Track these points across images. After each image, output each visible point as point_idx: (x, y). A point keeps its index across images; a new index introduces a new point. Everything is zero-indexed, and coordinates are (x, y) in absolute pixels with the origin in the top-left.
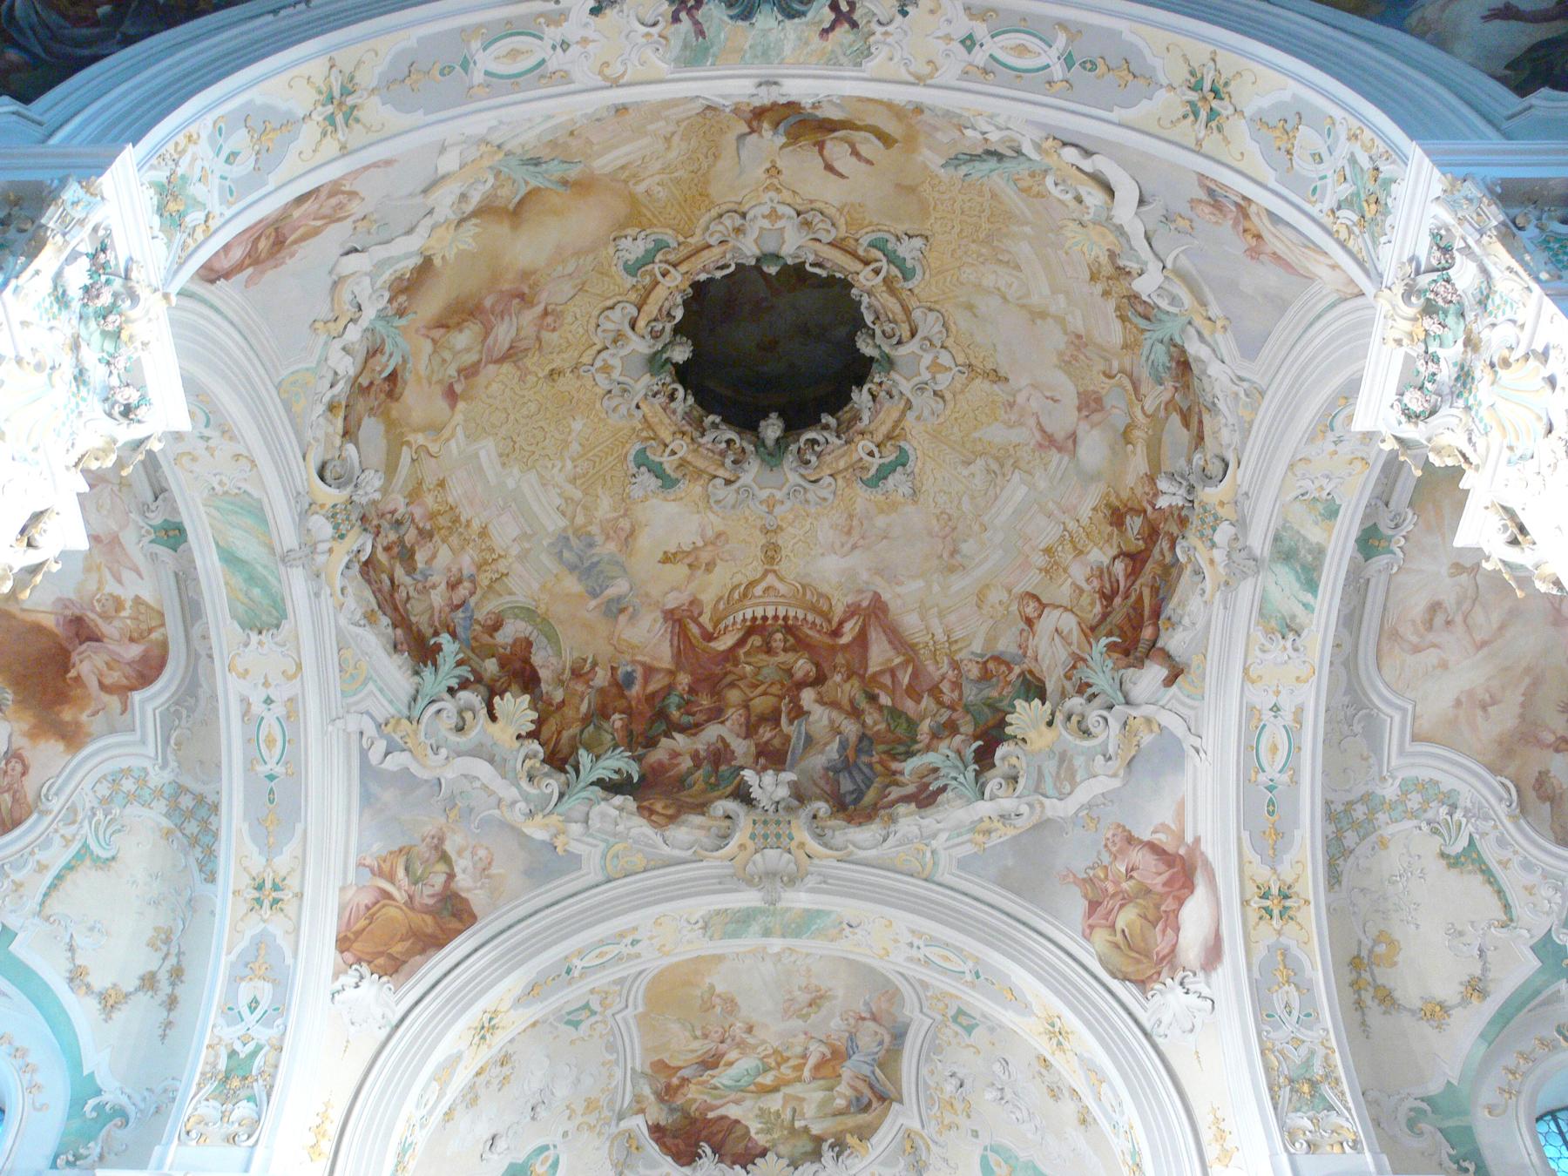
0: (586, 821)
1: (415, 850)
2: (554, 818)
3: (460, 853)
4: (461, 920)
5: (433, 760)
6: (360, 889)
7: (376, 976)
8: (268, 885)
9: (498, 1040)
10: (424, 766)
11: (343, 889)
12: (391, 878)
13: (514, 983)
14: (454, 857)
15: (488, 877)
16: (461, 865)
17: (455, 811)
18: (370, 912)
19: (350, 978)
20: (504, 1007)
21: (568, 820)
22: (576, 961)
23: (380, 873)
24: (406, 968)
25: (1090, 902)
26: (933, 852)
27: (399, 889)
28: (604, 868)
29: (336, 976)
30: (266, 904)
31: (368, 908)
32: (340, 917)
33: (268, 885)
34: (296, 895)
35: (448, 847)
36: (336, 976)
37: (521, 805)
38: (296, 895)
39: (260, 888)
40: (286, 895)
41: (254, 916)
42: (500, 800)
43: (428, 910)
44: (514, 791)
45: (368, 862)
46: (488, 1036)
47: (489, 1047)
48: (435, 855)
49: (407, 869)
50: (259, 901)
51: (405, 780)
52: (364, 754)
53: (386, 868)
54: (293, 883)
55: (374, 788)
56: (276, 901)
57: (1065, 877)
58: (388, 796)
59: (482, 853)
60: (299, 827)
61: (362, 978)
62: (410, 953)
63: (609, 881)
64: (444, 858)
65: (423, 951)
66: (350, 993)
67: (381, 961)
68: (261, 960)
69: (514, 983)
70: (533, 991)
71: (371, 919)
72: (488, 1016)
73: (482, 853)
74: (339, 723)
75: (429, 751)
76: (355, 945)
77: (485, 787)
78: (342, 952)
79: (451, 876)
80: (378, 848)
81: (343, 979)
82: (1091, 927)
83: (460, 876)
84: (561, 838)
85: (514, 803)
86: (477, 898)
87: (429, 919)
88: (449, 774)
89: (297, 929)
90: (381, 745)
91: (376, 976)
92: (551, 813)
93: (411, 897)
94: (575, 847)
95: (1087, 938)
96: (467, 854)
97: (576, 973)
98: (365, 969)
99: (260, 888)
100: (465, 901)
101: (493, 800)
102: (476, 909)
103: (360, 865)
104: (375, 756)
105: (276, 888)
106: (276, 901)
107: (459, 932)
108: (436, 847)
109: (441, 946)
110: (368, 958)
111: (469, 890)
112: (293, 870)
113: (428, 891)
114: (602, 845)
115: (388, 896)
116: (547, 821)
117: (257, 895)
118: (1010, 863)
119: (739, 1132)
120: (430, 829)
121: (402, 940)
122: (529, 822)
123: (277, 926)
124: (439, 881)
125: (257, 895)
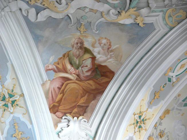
0: (148, 6)
1: (71, 53)
2: (132, 11)
3: (93, 46)
4: (107, 76)
5: (60, 8)
6: (52, 81)
7: (75, 118)
8: (7, 96)
9: (149, 125)
10: (57, 12)
11: (43, 85)
12: (65, 71)
13: (143, 97)
14: (91, 49)
15: (112, 51)
16: (96, 51)
17: (82, 27)
18: (61, 89)
19: (63, 124)
20: (144, 108)
21: (139, 9)
22: (171, 74)
23: (58, 70)
24: (89, 109)
27: (71, 74)
28: (166, 24)
29: (56, 125)
30: (10, 105)
31: (59, 88)
32: (47, 98)
33: (7, 96)
34: (21, 96)
35: (86, 45)
36: (56, 125)
37: (113, 11)
38: (21, 96)
39: (4, 99)
40: (17, 97)
41: (6, 113)
42: (102, 13)
43: (88, 78)
44: (107, 6)
45: (51, 67)
46: (142, 125)
47: (146, 130)
48: (81, 52)
49: (71, 64)
50: (6, 105)
51: (52, 22)
52: (26, 18)
53: (60, 66)
54: (17, 91)
55: (38, 32)
56: (13, 102)
58: (47, 33)
59: (104, 41)
60: (9, 64)
61: (69, 121)
62: (88, 101)
63: (171, 29)
64: (87, 51)
65: (94, 98)
66: (66, 130)
67: (76, 110)
68: (17, 131)
69: (143, 97)
70: (156, 96)
71: (63, 93)
72: (137, 117)
73: (104, 41)
74: (7, 9)
75: (56, 4)
76: (60, 108)
77: (91, 10)
78: (55, 113)
79: (94, 58)
80: (52, 59)
81: (60, 125)
83: (98, 57)
84: (138, 18)
85: (109, 11)
86: (110, 63)
87: (91, 82)
88: (71, 11)
89: (27, 110)
90: (33, 11)
91: (75, 118)
92: (129, 8)
93: (78, 75)
94: (148, 20)
96: (97, 45)
97: (174, 80)
98: (69, 117)
99: (4, 99)
101: (98, 14)
102: (112, 68)
103: (47, 70)
104: (32, 17)
105: (11, 96)
106: (13, 102)
107: (108, 83)
108: (81, 48)
109: (101, 92)
110: (69, 111)
111: (105, 61)
112: (15, 85)
114: (161, 14)
115: (68, 79)
116: (128, 13)
117: (3, 103)
120: (74, 41)
121: (82, 97)
122: (120, 17)
123: (18, 113)
124: (88, 63)
125: (3, 103)
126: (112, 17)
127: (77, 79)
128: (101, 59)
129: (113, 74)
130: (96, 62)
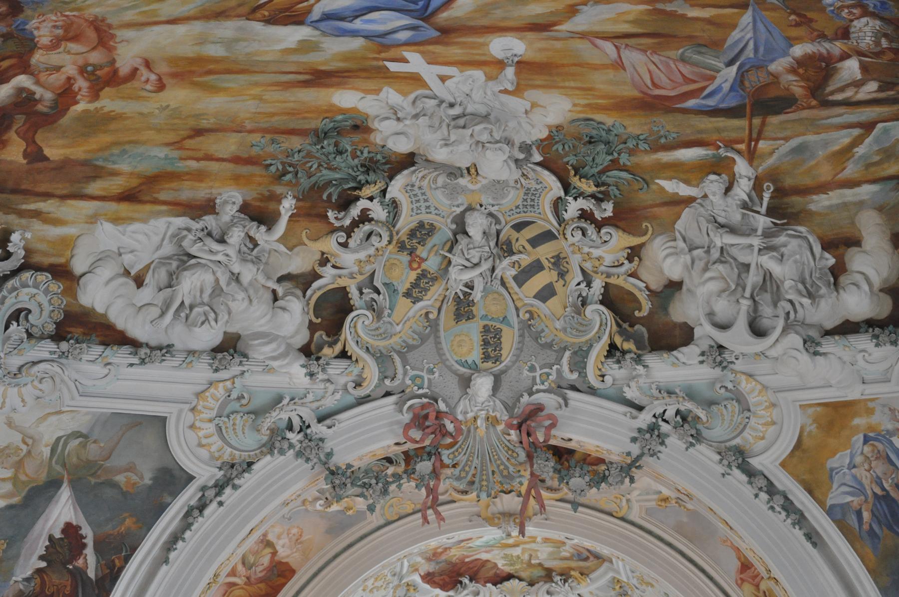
3: (279, 537)
14: (274, 541)
15: (300, 543)
25: (742, 564)
26: (628, 501)
27: (240, 577)
35: (270, 537)
43: (261, 580)
57: (725, 541)
64: (269, 544)
79: (274, 553)
82: (743, 580)
87: (262, 586)
93: (248, 578)
95: (740, 586)
100: (287, 563)
102: (294, 566)
107: (284, 585)
111: (288, 556)
113: (261, 568)
118: (685, 520)
119: (489, 565)
124: (266, 560)
126: (319, 505)
127: (245, 584)
128: (284, 554)
129: (293, 572)
130: (276, 558)
